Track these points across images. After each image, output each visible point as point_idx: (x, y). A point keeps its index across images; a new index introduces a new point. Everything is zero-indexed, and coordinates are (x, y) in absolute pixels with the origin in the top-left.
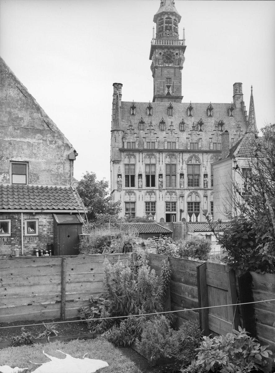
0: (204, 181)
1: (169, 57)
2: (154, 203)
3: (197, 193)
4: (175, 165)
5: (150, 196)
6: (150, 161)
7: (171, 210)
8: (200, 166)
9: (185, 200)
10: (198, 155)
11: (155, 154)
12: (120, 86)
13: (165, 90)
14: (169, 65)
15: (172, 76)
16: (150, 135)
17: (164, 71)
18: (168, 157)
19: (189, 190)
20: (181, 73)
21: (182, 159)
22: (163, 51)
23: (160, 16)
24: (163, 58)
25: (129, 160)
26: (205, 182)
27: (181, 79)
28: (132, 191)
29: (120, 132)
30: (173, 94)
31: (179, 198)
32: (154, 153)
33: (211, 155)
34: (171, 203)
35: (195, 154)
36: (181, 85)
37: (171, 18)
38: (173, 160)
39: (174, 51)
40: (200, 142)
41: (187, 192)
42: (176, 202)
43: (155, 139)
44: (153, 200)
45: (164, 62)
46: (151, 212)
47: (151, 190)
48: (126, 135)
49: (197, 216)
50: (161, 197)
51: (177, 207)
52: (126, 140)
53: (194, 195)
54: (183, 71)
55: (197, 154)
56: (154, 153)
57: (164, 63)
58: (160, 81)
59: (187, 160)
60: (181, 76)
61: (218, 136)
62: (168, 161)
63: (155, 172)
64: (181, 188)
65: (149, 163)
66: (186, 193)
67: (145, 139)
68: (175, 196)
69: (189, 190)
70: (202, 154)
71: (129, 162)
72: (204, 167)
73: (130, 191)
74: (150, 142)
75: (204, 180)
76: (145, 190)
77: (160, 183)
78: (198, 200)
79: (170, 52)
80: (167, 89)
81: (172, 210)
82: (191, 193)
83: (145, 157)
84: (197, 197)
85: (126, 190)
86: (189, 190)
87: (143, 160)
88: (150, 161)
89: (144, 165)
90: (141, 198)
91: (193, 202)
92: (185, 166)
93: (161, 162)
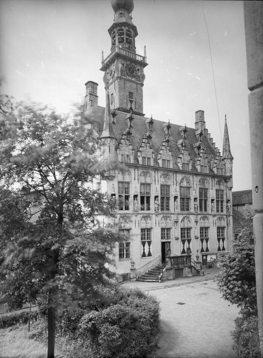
0: (195, 205)
1: (131, 70)
2: (149, 230)
3: (188, 218)
4: (168, 186)
6: (145, 179)
7: (166, 238)
8: (191, 188)
10: (189, 177)
11: (151, 172)
13: (128, 104)
15: (134, 91)
16: (146, 149)
18: (162, 176)
19: (183, 214)
21: (176, 180)
22: (126, 63)
23: (121, 26)
24: (126, 70)
26: (196, 207)
27: (142, 96)
28: (127, 215)
29: (114, 140)
30: (136, 110)
31: (174, 223)
32: (149, 171)
33: (199, 178)
35: (187, 175)
36: (143, 103)
37: (131, 32)
38: (167, 180)
42: (171, 228)
43: (151, 155)
44: (149, 226)
45: (127, 74)
46: (146, 240)
48: (120, 145)
49: (189, 244)
51: (171, 233)
52: (121, 152)
53: (186, 220)
54: (144, 88)
55: (188, 176)
56: (149, 171)
59: (179, 181)
60: (142, 94)
62: (162, 181)
63: (149, 193)
64: (176, 213)
65: (143, 182)
66: (181, 217)
67: (141, 153)
68: (169, 222)
70: (192, 176)
71: (123, 179)
72: (194, 190)
73: (125, 215)
74: (145, 158)
75: (195, 204)
76: (141, 214)
77: (157, 206)
78: (189, 226)
79: (133, 66)
80: (129, 103)
81: (167, 239)
82: (184, 218)
83: (140, 175)
85: (120, 214)
87: (139, 178)
88: (145, 179)
89: (139, 184)
90: (137, 224)
91: (185, 228)
92: (178, 188)
93: (157, 182)
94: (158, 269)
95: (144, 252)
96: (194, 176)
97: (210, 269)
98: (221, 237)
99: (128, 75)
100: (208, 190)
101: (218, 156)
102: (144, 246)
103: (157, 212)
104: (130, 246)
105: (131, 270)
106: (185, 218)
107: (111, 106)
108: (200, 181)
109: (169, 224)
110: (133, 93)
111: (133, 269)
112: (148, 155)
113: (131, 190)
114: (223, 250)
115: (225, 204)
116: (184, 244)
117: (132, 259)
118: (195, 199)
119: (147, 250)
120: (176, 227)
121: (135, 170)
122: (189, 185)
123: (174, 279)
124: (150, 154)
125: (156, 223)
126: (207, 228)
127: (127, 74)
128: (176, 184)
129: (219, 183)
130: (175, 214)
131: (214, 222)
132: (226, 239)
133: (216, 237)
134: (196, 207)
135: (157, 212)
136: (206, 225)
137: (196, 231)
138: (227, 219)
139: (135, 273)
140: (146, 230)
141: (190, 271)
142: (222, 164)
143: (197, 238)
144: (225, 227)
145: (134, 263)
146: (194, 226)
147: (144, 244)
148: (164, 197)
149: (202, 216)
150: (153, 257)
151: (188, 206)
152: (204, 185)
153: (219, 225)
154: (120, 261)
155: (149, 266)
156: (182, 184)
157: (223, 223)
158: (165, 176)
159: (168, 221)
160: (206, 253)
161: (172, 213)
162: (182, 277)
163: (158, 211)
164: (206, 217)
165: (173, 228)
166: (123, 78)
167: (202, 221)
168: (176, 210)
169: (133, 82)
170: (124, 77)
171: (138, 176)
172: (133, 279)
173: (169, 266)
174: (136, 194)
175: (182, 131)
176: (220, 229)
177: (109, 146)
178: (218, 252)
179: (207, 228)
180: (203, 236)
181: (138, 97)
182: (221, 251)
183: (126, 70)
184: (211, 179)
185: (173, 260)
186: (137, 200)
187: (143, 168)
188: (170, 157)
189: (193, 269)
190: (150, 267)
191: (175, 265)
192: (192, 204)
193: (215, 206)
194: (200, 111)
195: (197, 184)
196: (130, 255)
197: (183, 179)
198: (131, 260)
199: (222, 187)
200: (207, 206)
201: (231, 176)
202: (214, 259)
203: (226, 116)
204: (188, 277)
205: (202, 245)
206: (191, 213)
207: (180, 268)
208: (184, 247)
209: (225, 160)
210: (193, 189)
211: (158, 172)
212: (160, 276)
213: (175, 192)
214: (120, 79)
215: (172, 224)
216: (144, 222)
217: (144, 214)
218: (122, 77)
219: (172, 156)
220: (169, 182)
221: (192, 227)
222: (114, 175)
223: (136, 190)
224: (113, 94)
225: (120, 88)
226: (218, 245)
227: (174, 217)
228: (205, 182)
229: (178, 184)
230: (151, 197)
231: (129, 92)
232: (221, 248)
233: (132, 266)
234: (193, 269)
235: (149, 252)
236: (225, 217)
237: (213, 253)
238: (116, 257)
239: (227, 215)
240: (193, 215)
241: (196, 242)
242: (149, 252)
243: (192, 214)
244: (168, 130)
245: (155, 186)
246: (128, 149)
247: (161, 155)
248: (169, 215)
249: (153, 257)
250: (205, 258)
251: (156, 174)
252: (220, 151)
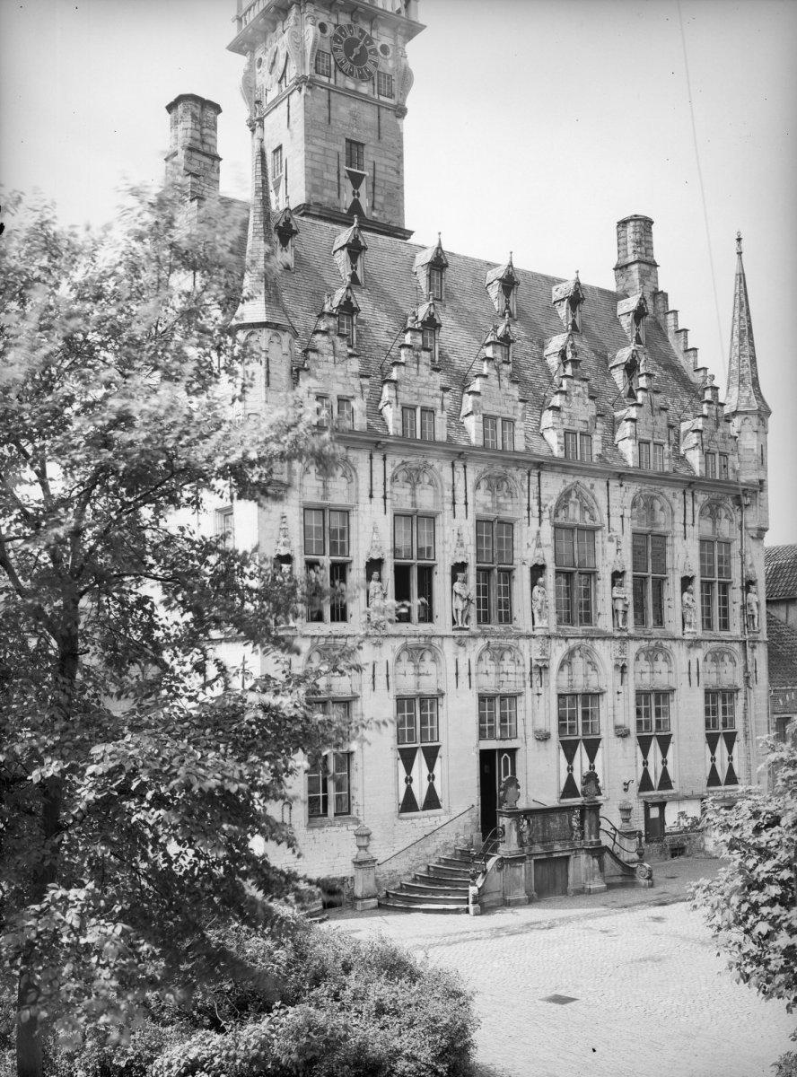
0: (614, 599)
1: (356, 51)
2: (429, 702)
4: (509, 525)
5: (417, 667)
6: (413, 495)
8: (599, 534)
9: (553, 684)
10: (592, 486)
11: (437, 465)
12: (210, 113)
13: (342, 188)
14: (357, 84)
16: (414, 372)
17: (337, 109)
18: (483, 484)
20: (401, 135)
21: (539, 498)
24: (336, 50)
25: (320, 484)
26: (620, 606)
27: (400, 156)
28: (341, 641)
29: (286, 337)
30: (374, 214)
31: (531, 673)
33: (633, 489)
34: (497, 700)
35: (580, 479)
38: (501, 500)
39: (374, 35)
42: (520, 694)
43: (436, 396)
44: (428, 687)
45: (339, 66)
46: (418, 745)
47: (422, 639)
48: (312, 355)
49: (592, 757)
50: (463, 671)
51: (520, 715)
53: (578, 662)
54: (408, 125)
55: (587, 482)
56: (430, 463)
57: (339, 74)
58: (324, 144)
59: (552, 503)
60: (401, 147)
61: (655, 413)
62: (482, 500)
64: (537, 632)
65: (406, 506)
66: (558, 651)
67: (396, 389)
68: (511, 669)
69: (563, 641)
71: (325, 496)
72: (611, 540)
73: (331, 641)
74: (413, 409)
75: (616, 595)
77: (460, 605)
78: (594, 683)
82: (571, 653)
83: (394, 478)
84: (590, 667)
87: (388, 489)
88: (413, 495)
89: (390, 516)
90: (381, 679)
91: (577, 695)
92: (547, 530)
93: (460, 507)
94: (467, 859)
95: (409, 792)
96: (614, 483)
97: (676, 860)
98: (721, 730)
99: (341, 70)
100: (669, 541)
101: (709, 402)
102: (408, 768)
103: (461, 629)
104: (353, 765)
105: (359, 864)
106: (577, 654)
107: (272, 196)
108: (634, 505)
109: (511, 677)
110: (363, 145)
111: (366, 862)
112: (426, 399)
113: (358, 540)
114: (727, 783)
115: (735, 595)
116: (570, 758)
117: (361, 818)
118: (617, 576)
119: (421, 783)
120: (541, 690)
121: (371, 458)
122: (592, 518)
123: (530, 901)
124: (435, 392)
125: (457, 674)
126: (664, 695)
127: (339, 66)
128: (540, 517)
129: (712, 511)
130: (534, 637)
131: (694, 670)
132: (740, 736)
133: (700, 731)
134: (620, 606)
135: (461, 629)
136: (662, 681)
137: (620, 704)
138: (746, 657)
139: (372, 875)
140: (417, 702)
141: (597, 869)
142: (723, 436)
143: (623, 734)
144: (737, 690)
145: (368, 835)
146: (610, 683)
147: (407, 757)
148: (492, 569)
149: (644, 643)
150: (448, 812)
151: (587, 605)
152: (653, 518)
153: (711, 680)
154: (310, 826)
155: (430, 850)
156: (562, 513)
157: (731, 675)
158: (496, 483)
159: (507, 665)
160: (662, 796)
161: (524, 631)
162: (565, 892)
163: (466, 626)
164: (659, 649)
165: (528, 692)
166: (323, 83)
167: (644, 665)
168: (540, 618)
169: (364, 99)
170: (325, 79)
171: (385, 484)
172: (365, 901)
173: (509, 846)
174: (376, 557)
175: (563, 300)
176: (718, 698)
177: (268, 360)
178: (708, 792)
179: (664, 695)
180: (647, 727)
181: (386, 162)
182: (723, 788)
183: (336, 50)
184: (680, 495)
185: (529, 821)
186: (380, 580)
187: (406, 450)
188: (513, 403)
189: (607, 858)
190: (435, 852)
191: (533, 843)
192: (604, 595)
193: (698, 605)
194: (635, 218)
195: (622, 516)
196: (352, 802)
197: (567, 494)
198: (357, 822)
199: (726, 528)
200: (666, 604)
201: (761, 482)
202: (694, 819)
203: (739, 240)
204: (590, 892)
205: (646, 763)
206: (600, 632)
207: (555, 855)
208: (570, 769)
209: (737, 421)
210: (608, 535)
211: (465, 467)
212: (473, 890)
213: (533, 545)
214: (309, 87)
215: (522, 679)
216: (410, 668)
217: (410, 636)
218: (317, 77)
219: (521, 401)
220: (509, 507)
221: (605, 688)
222: (285, 478)
223: (375, 538)
224: (280, 148)
225: (310, 125)
226: (709, 764)
227: (529, 651)
228: (658, 506)
229: (546, 515)
230: (436, 569)
231: (347, 140)
232: (722, 775)
233: (359, 847)
234: (607, 858)
235: (431, 790)
236: (737, 647)
237: (688, 793)
238: (293, 812)
239: (745, 642)
240: (607, 642)
241: (621, 749)
242: (431, 790)
243: (605, 637)
244: (508, 296)
245: (456, 521)
246: (342, 374)
247: (477, 398)
248: (511, 642)
249: (447, 813)
250: (654, 813)
251: (456, 474)
252: (715, 383)
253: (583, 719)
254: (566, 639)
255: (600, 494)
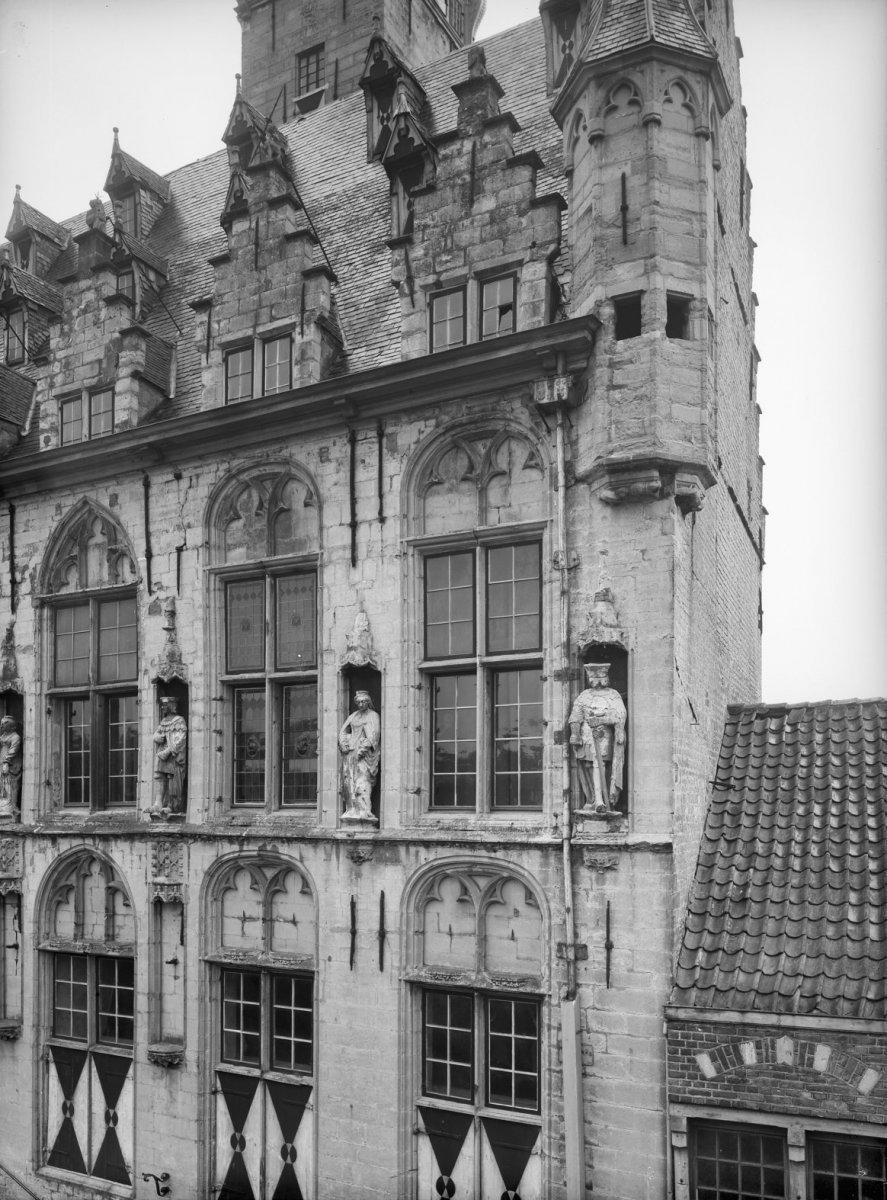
40: (124, 371)
41: (38, 857)
86: (54, 838)
131: (368, 924)
240: (138, 844)
241: (163, 1093)
253: (257, 1040)
254: (54, 838)
255: (130, 516)
